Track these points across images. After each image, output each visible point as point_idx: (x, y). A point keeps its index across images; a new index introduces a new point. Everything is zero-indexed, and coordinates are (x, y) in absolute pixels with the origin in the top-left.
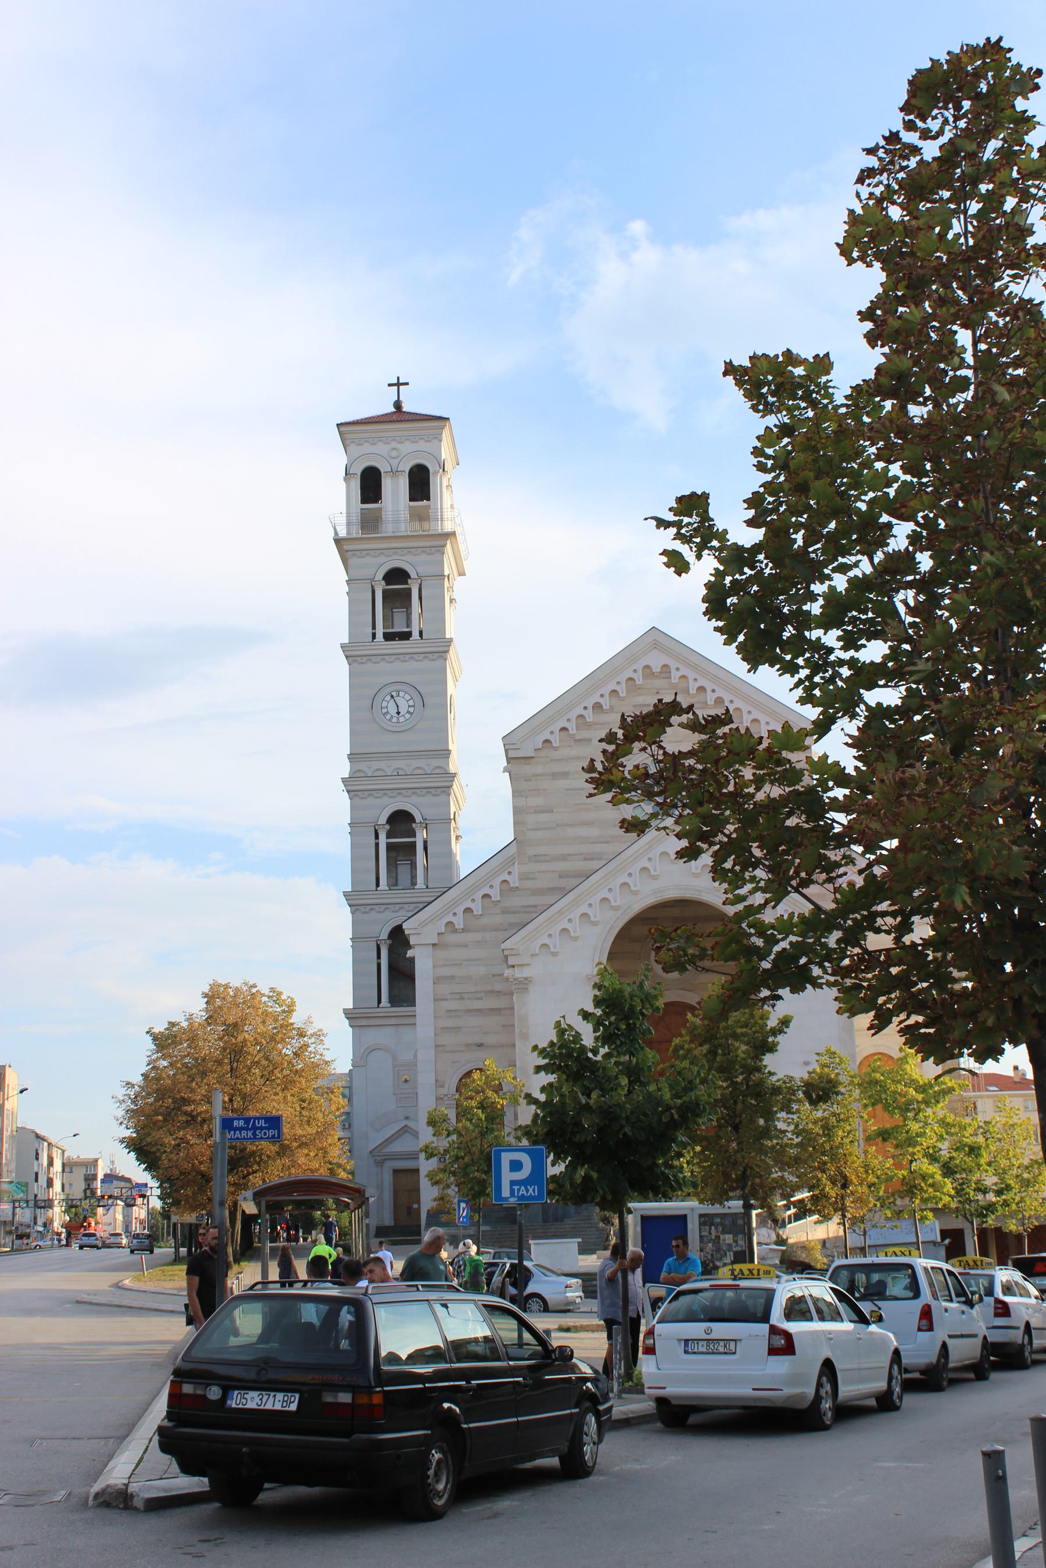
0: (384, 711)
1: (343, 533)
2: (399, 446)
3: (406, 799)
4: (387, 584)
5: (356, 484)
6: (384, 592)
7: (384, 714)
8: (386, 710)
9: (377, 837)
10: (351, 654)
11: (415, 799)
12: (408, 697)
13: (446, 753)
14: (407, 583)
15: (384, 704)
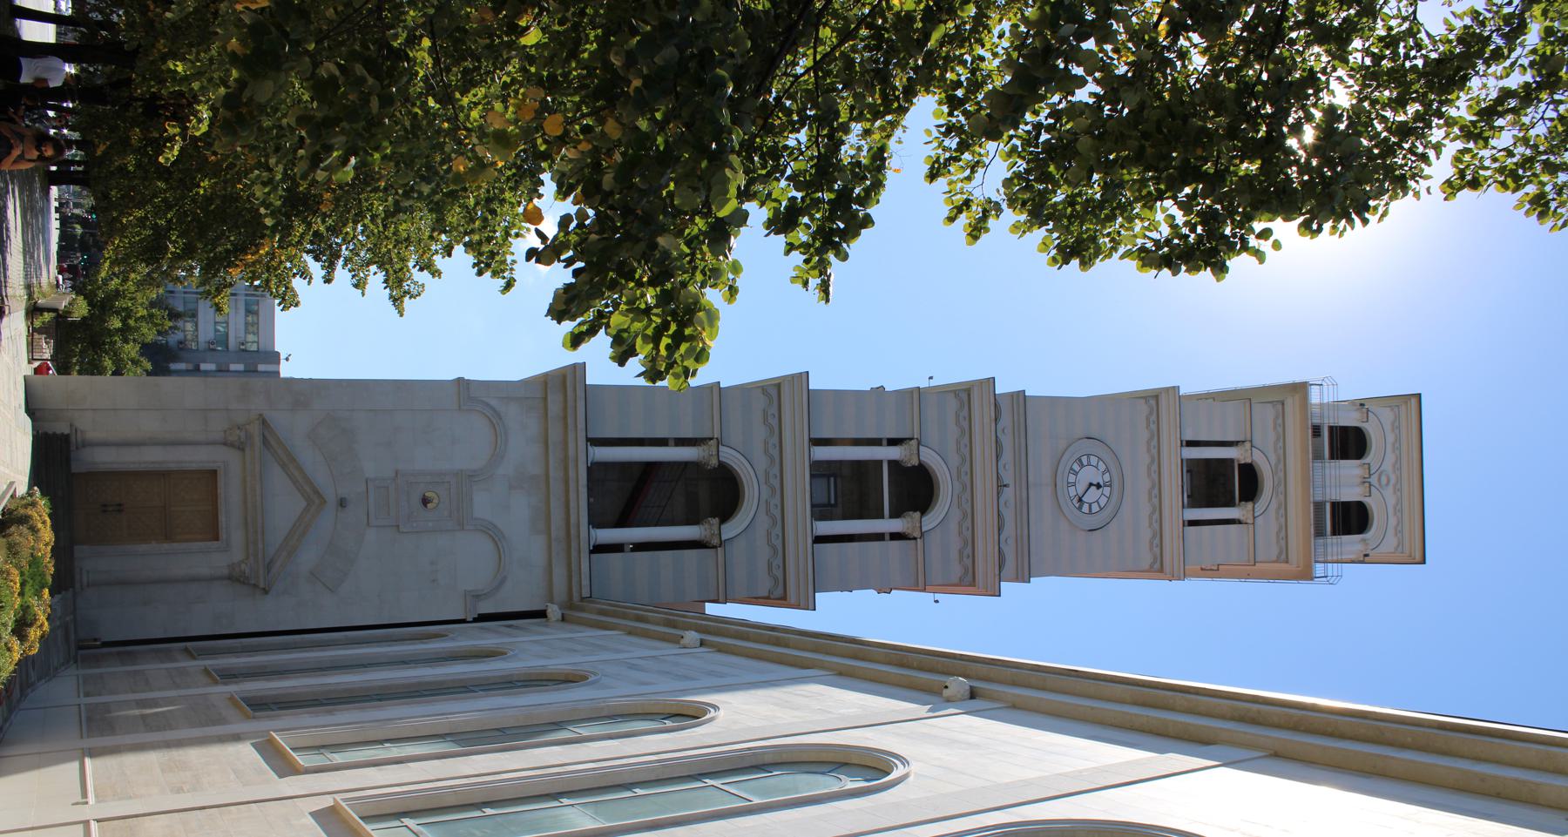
0: (1084, 460)
1: (1315, 397)
2: (1391, 487)
3: (955, 498)
4: (1239, 465)
5: (1349, 420)
6: (1228, 463)
7: (1080, 460)
8: (1085, 463)
9: (893, 442)
10: (1155, 400)
11: (763, 522)
12: (1103, 501)
13: (1023, 576)
14: (1240, 501)
15: (1094, 460)
